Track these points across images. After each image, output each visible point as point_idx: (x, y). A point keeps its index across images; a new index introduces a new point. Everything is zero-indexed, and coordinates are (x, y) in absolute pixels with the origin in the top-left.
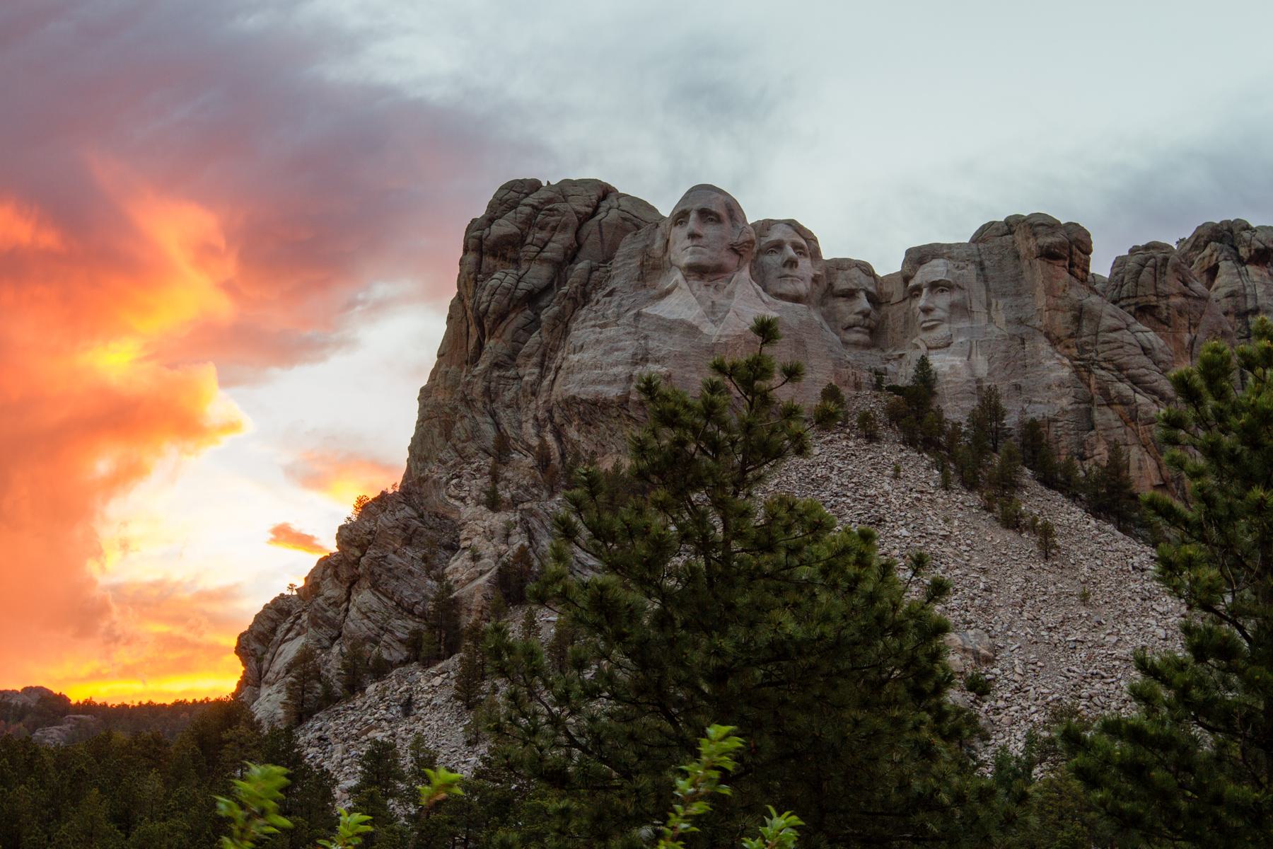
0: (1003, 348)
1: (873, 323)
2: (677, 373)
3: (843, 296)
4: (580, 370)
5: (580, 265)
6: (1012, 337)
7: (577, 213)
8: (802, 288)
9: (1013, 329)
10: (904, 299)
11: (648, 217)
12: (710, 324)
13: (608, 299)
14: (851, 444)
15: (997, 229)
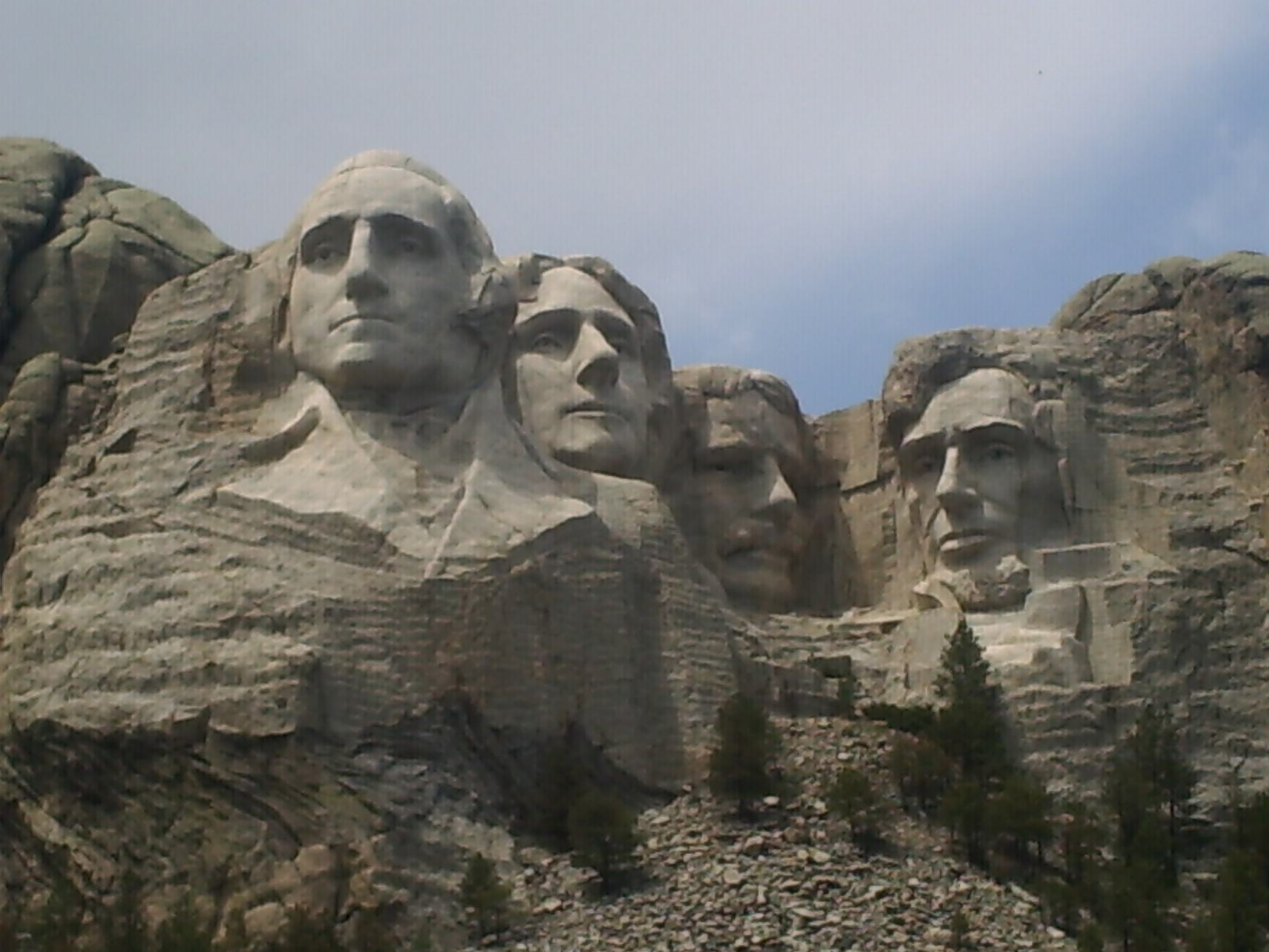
0: (1167, 606)
1: (797, 543)
2: (337, 658)
3: (720, 468)
4: (62, 651)
5: (32, 367)
6: (1192, 578)
7: (9, 225)
8: (631, 438)
9: (1194, 557)
10: (883, 479)
11: (187, 243)
12: (417, 529)
13: (114, 458)
14: (820, 855)
15: (1130, 294)
